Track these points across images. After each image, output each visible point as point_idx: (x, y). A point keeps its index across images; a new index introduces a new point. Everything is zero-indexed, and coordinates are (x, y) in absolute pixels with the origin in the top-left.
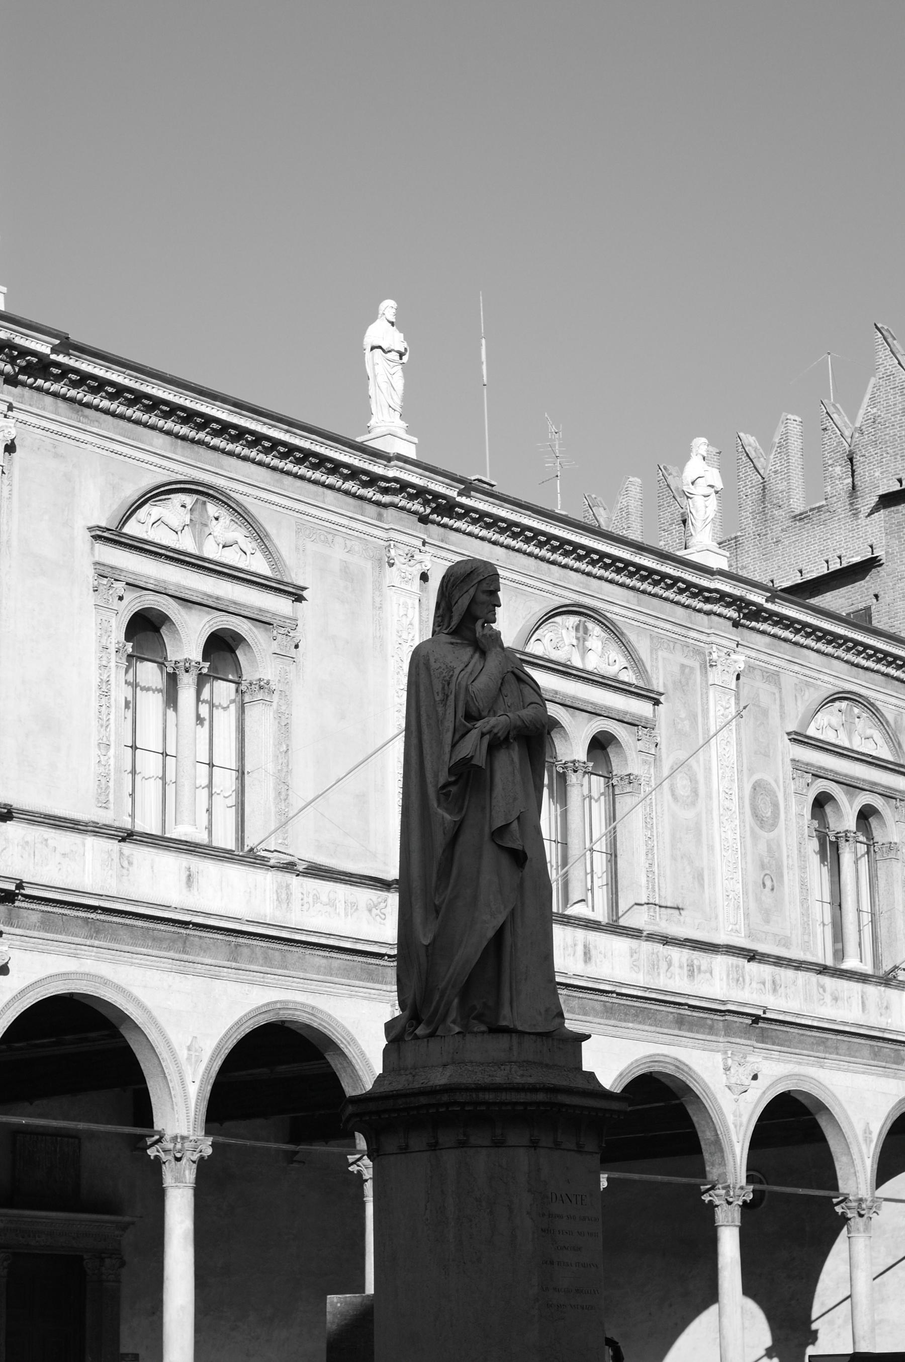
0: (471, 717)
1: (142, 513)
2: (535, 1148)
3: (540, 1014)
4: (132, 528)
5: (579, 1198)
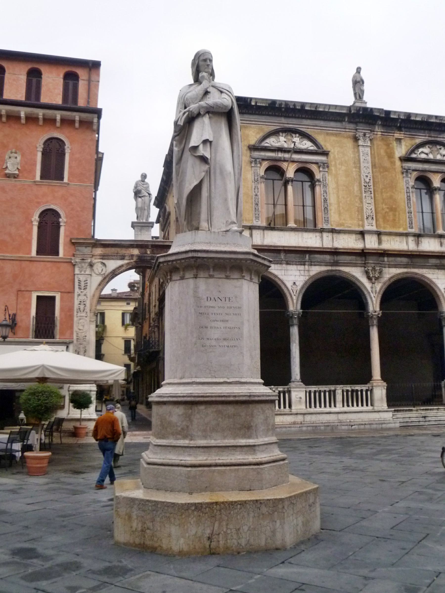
0: (185, 108)
1: (416, 152)
2: (196, 278)
3: (224, 224)
4: (414, 156)
5: (227, 300)
